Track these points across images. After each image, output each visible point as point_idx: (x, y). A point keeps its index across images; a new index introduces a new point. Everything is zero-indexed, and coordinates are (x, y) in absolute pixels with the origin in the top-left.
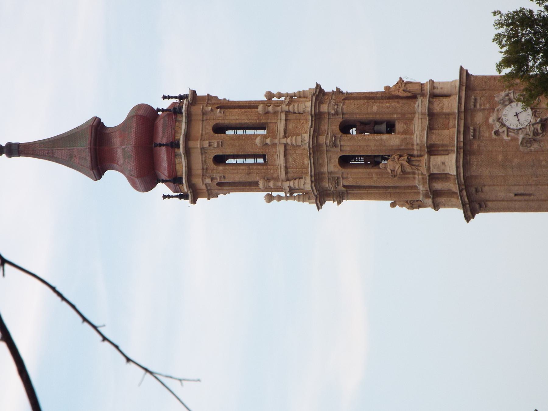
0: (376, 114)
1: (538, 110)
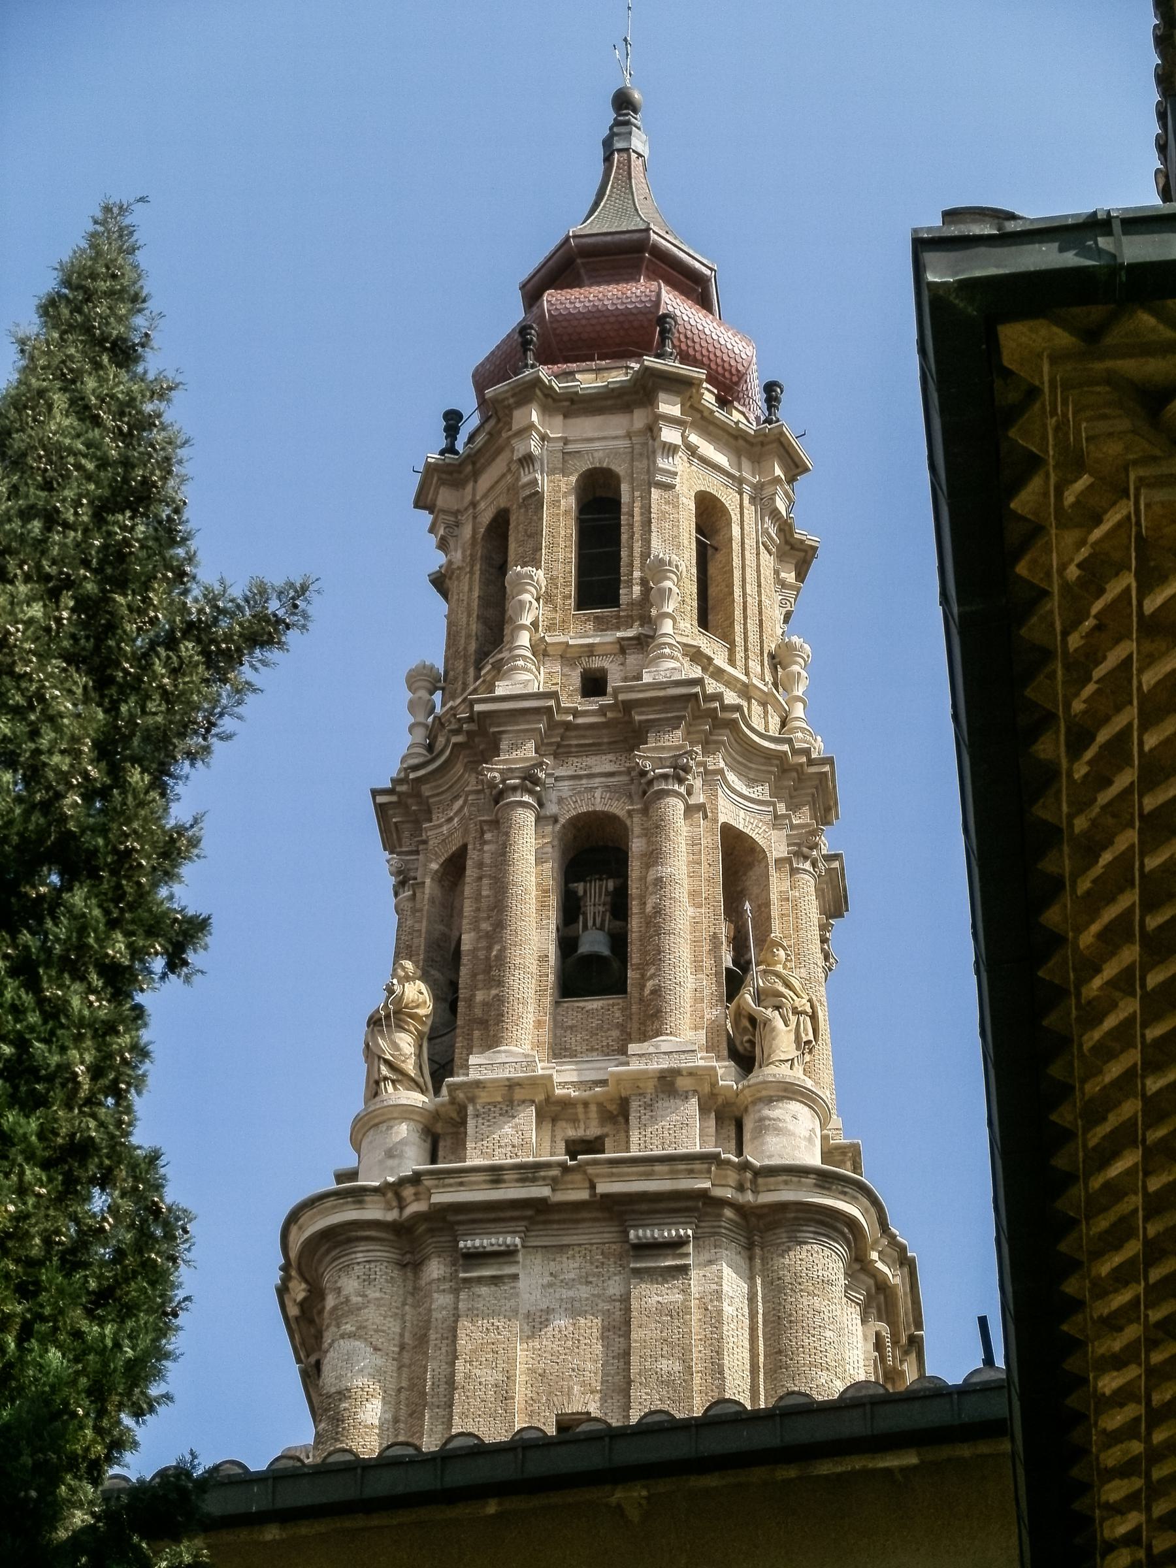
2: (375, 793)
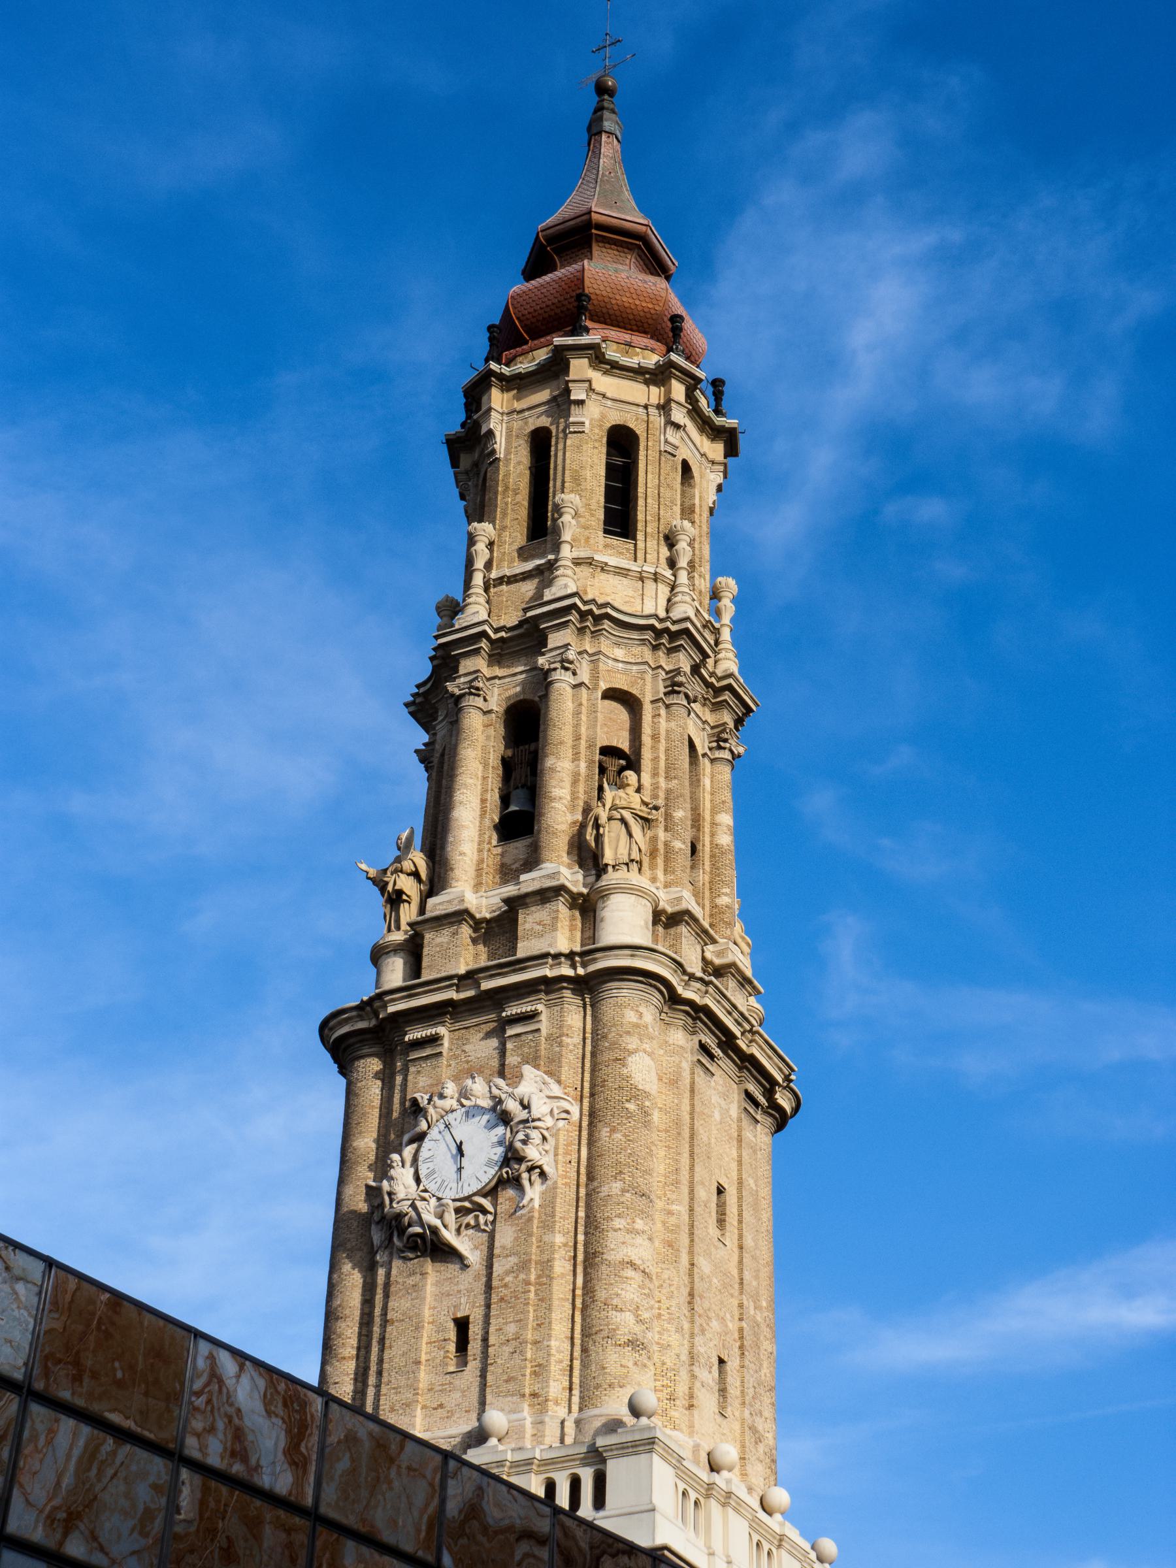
1: (490, 1218)
2: (407, 705)
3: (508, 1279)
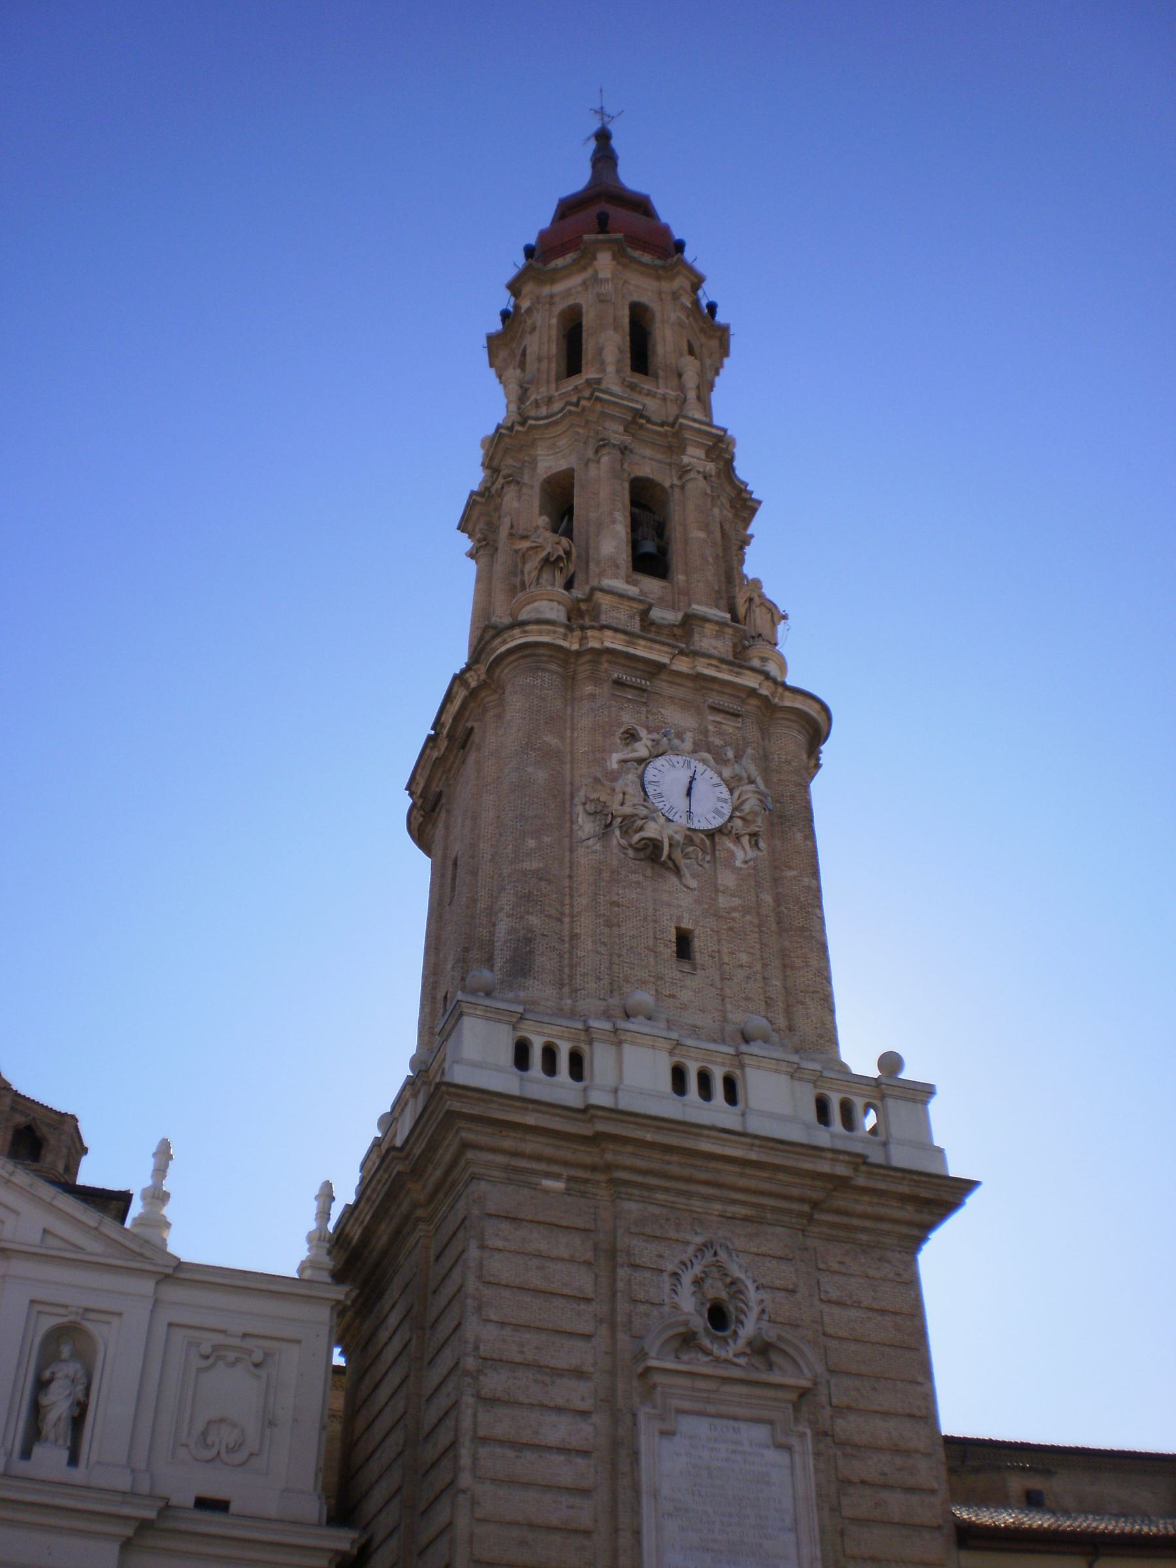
0: (686, 541)
1: (708, 858)
3: (735, 915)
